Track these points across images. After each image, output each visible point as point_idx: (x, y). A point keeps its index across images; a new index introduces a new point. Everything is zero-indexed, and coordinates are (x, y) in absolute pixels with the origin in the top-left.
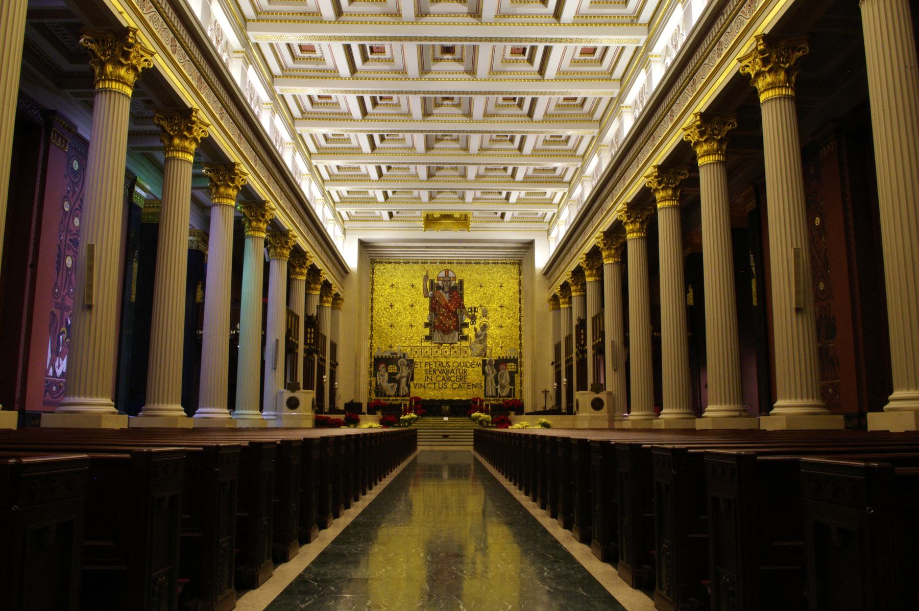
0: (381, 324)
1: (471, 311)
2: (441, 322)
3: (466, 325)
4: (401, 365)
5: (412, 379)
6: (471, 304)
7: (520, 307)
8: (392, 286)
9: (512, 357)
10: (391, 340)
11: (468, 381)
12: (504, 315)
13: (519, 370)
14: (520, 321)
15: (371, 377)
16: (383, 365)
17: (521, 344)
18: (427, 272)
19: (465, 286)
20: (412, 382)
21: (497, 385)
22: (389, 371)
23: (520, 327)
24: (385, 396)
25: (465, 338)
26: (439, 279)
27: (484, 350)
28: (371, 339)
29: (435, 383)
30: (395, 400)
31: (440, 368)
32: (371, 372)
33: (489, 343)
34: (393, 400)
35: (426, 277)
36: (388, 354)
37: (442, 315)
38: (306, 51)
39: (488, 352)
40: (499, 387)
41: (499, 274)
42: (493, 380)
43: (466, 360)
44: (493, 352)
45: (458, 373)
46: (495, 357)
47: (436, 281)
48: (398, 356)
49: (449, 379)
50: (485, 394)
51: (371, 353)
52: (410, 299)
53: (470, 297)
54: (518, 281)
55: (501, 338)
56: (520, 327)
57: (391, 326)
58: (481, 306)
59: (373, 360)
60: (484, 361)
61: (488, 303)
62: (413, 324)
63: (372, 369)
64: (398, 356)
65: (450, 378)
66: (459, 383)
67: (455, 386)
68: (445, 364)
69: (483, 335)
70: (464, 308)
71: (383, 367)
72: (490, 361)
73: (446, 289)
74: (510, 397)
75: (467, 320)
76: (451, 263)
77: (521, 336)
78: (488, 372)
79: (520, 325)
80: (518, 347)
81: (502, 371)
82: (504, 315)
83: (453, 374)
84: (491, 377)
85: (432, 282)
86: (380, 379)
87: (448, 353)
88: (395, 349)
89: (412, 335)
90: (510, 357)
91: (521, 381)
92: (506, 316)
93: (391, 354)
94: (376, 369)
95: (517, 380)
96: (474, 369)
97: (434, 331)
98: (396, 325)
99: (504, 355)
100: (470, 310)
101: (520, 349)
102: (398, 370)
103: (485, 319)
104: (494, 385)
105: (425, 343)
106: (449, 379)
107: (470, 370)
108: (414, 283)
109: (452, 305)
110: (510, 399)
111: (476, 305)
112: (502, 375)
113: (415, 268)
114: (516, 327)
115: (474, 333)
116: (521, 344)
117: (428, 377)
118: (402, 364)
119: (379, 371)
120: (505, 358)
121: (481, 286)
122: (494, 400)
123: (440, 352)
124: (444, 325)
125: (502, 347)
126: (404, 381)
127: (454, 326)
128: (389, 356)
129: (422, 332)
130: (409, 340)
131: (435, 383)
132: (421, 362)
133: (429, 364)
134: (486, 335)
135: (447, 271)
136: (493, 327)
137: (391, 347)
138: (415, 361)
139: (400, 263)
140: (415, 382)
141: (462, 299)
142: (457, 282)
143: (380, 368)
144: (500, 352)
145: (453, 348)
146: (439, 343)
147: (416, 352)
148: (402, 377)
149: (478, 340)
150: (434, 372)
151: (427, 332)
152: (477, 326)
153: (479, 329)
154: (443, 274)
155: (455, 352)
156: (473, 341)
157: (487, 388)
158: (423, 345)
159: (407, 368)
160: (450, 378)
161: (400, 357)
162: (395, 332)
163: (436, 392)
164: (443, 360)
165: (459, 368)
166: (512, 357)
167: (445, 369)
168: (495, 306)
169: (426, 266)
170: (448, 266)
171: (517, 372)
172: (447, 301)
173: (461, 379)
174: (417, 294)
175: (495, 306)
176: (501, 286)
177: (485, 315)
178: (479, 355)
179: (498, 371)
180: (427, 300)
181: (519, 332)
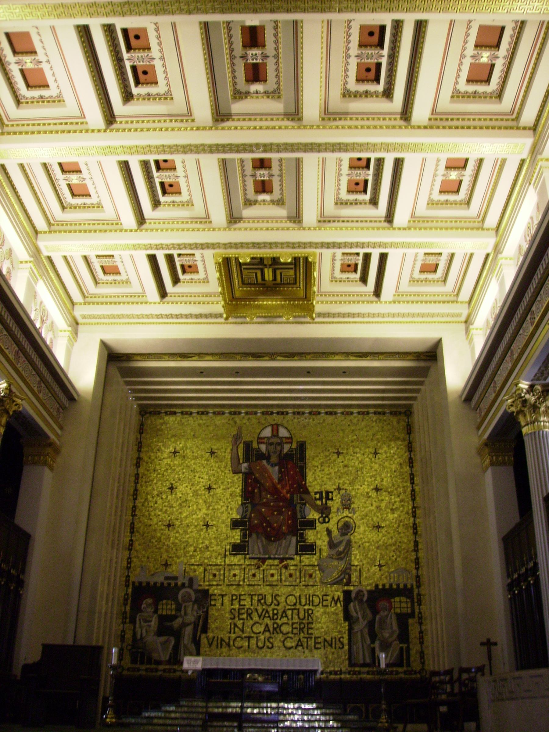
0: (150, 522)
1: (321, 499)
2: (263, 518)
3: (311, 524)
4: (184, 601)
5: (205, 630)
6: (321, 486)
7: (413, 490)
8: (175, 453)
9: (402, 586)
10: (167, 551)
11: (316, 633)
12: (383, 505)
13: (417, 611)
14: (414, 516)
15: (124, 623)
16: (150, 601)
17: (417, 559)
18: (240, 429)
19: (309, 453)
20: (203, 636)
21: (373, 642)
22: (160, 612)
23: (415, 527)
24: (149, 662)
25: (310, 549)
26: (260, 440)
27: (347, 572)
28: (130, 550)
29: (249, 638)
30: (170, 671)
31: (260, 609)
32: (125, 612)
33: (356, 558)
34: (164, 671)
35: (237, 438)
36: (160, 579)
37: (266, 505)
38: (79, 196)
39: (354, 578)
40: (377, 645)
41: (371, 433)
42: (366, 630)
44: (364, 575)
45: (295, 617)
46: (367, 585)
47: (255, 445)
48: (179, 583)
49: (277, 629)
50: (350, 659)
51: (128, 576)
52: (206, 477)
53: (318, 473)
54: (406, 443)
55: (378, 548)
56: (415, 527)
57: (169, 526)
58: (339, 489)
59: (130, 590)
60: (347, 594)
61: (352, 483)
62: (210, 523)
63: (128, 608)
64: (179, 583)
65: (280, 626)
66: (297, 638)
67: (289, 644)
68: (269, 599)
69: (344, 544)
70: (307, 492)
71: (150, 605)
72: (359, 592)
73: (274, 459)
74: (400, 665)
75: (314, 515)
76: (282, 413)
77: (416, 543)
78: (354, 614)
79: (415, 524)
80: (413, 565)
81: (383, 614)
82: (383, 505)
83: (285, 620)
84: (361, 625)
85: (248, 446)
86: (141, 627)
87: (276, 578)
89: (207, 542)
90: (398, 585)
91: (421, 632)
92: (386, 507)
93: (167, 578)
94: (136, 607)
95: (414, 632)
96: (329, 610)
97: (250, 536)
98: (177, 523)
99: (385, 581)
100: (318, 496)
101: (417, 569)
102: (178, 609)
103: (346, 513)
104: (368, 642)
105: (232, 558)
106: (277, 629)
107: (319, 611)
108: (214, 447)
109: (283, 487)
110: (400, 669)
111: (330, 487)
112: (382, 622)
113: (217, 423)
114: (406, 526)
115: (326, 539)
116: (417, 559)
117: (235, 625)
118: (188, 598)
119: (142, 611)
120: (387, 586)
121: (338, 453)
122: (368, 673)
123: (259, 576)
124: (269, 525)
125: (380, 566)
126: (189, 630)
127: (288, 526)
128: (162, 584)
129: (227, 537)
130: (201, 551)
131: (249, 638)
132: (223, 596)
133: (239, 598)
134: (349, 543)
135: (275, 428)
136: (362, 529)
137: (166, 565)
138: (211, 592)
139: (191, 413)
140: (211, 635)
141: (303, 476)
142: (294, 446)
143: (143, 606)
144: (378, 575)
145: (286, 567)
146: (259, 559)
147: (215, 575)
148: (184, 625)
149: (334, 552)
150: (249, 615)
151: (236, 536)
152: (332, 525)
153: (335, 532)
154: (267, 433)
155: (291, 575)
156: (325, 554)
157: (354, 648)
158: (227, 562)
159: (196, 607)
160: (280, 626)
161: (183, 585)
162: (176, 538)
163: (249, 655)
164: (266, 590)
165: (298, 606)
166: (402, 586)
167: (270, 609)
168: (365, 488)
169: (237, 418)
170: (278, 419)
171: (412, 615)
172: (276, 480)
173: (301, 630)
174: (218, 467)
175: (365, 488)
176: (376, 453)
177: (347, 505)
178: (338, 582)
179: (375, 611)
180: (238, 479)
181: (412, 537)
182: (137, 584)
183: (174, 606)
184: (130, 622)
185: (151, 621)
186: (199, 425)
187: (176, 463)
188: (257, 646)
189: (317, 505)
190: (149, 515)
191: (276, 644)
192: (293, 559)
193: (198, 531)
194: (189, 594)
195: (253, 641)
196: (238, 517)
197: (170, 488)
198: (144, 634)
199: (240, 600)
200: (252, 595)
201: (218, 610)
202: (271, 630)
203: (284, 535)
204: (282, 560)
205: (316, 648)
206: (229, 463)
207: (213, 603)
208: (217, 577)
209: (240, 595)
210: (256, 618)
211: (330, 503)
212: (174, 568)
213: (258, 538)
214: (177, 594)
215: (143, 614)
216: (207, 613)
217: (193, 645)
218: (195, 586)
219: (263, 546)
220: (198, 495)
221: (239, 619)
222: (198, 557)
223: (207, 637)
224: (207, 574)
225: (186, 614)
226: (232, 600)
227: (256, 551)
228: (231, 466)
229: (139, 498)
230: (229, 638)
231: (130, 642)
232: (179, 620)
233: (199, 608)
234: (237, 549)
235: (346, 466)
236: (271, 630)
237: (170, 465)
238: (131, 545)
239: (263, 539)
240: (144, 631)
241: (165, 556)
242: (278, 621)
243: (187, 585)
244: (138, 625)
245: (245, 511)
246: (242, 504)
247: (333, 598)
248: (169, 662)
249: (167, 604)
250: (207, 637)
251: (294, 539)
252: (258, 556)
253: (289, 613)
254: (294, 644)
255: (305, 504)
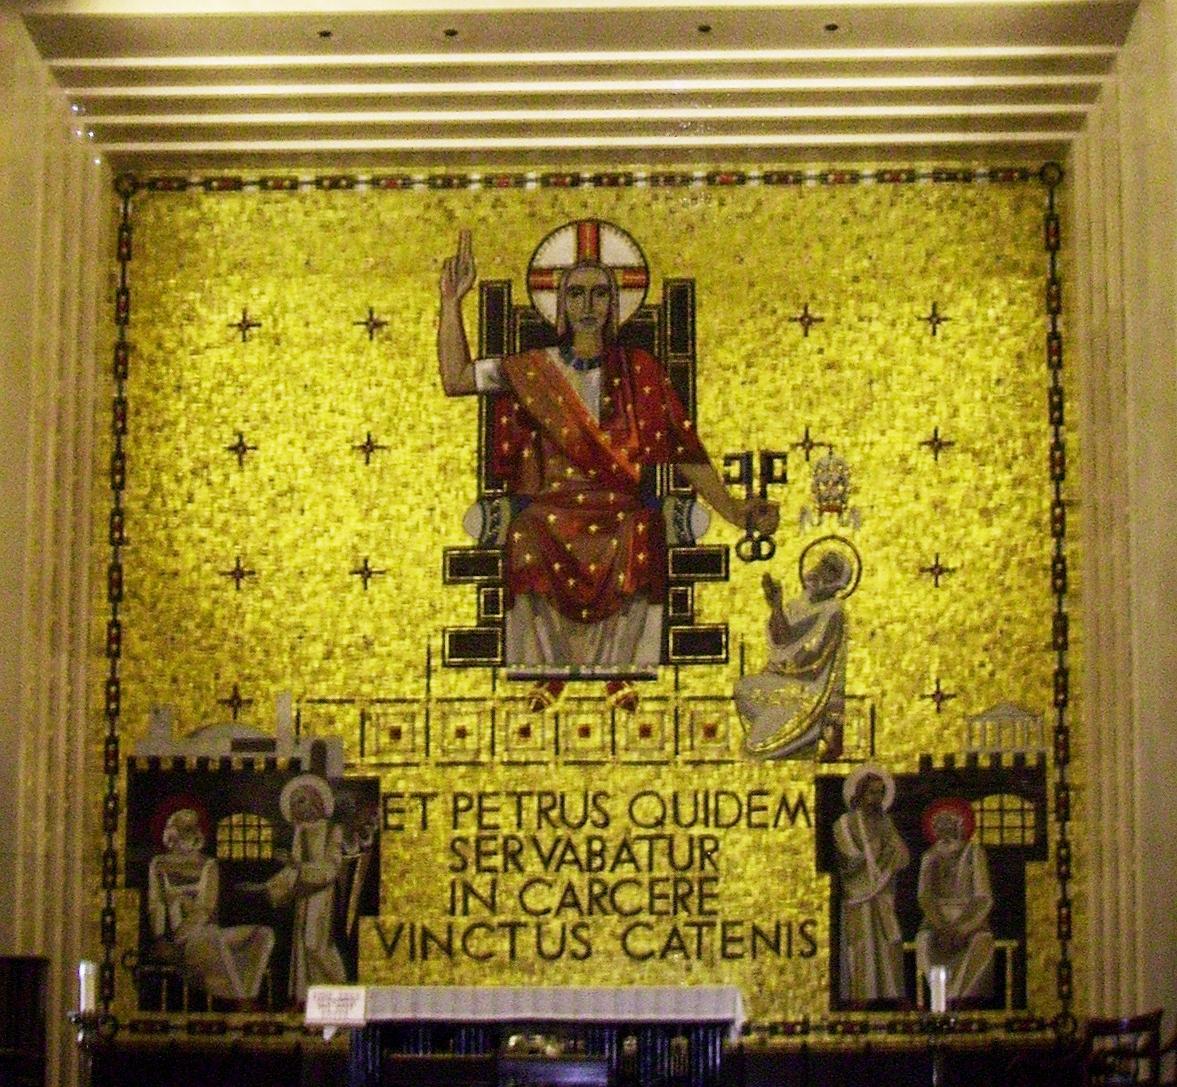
1: (746, 478)
2: (551, 546)
3: (713, 564)
4: (299, 817)
5: (371, 904)
8: (245, 325)
15: (109, 886)
16: (187, 816)
20: (366, 923)
22: (223, 851)
24: (199, 1002)
25: (708, 644)
26: (539, 281)
28: (115, 655)
29: (513, 927)
31: (546, 838)
32: (111, 854)
35: (457, 271)
36: (216, 748)
37: (562, 501)
43: (712, 779)
45: (662, 860)
47: (519, 296)
48: (282, 761)
49: (603, 899)
52: (355, 409)
57: (238, 574)
58: (808, 444)
59: (122, 784)
61: (850, 424)
62: (376, 563)
64: (282, 761)
66: (666, 927)
67: (640, 943)
68: (575, 809)
70: (699, 456)
73: (586, 343)
75: (719, 532)
76: (613, 181)
83: (627, 870)
86: (166, 900)
87: (595, 739)
88: (263, 718)
89: (367, 628)
93: (239, 745)
97: (510, 603)
98: (265, 565)
100: (735, 470)
102: (282, 841)
105: (452, 676)
107: (736, 844)
109: (617, 442)
111: (776, 439)
113: (386, 217)
117: (468, 889)
119: (164, 850)
121: (807, 322)
123: (542, 733)
124: (573, 567)
126: (318, 907)
127: (637, 572)
129: (434, 611)
131: (513, 927)
132: (424, 798)
137: (236, 702)
138: (385, 787)
139: (295, 185)
140: (390, 919)
141: (685, 400)
142: (655, 296)
146: (541, 679)
147: (396, 734)
148: (304, 890)
150: (512, 857)
151: (463, 607)
154: (561, 251)
158: (437, 691)
159: (338, 833)
161: (295, 766)
162: (264, 614)
163: (514, 980)
165: (669, 828)
167: (578, 838)
172: (594, 418)
173: (680, 900)
180: (465, 414)
182: (143, 765)
183: (267, 833)
184: (128, 885)
185: (196, 880)
186: (325, 226)
187: (252, 360)
188: (540, 952)
189: (732, 501)
190: (170, 539)
191: (598, 945)
192: (649, 677)
193: (335, 590)
194: (316, 793)
195: (527, 938)
196: (469, 542)
197: (233, 449)
198: (177, 921)
199: (481, 811)
200: (520, 796)
201: (410, 843)
202: (584, 902)
203: (623, 601)
204: (615, 682)
205: (725, 956)
206: (433, 359)
207: (393, 820)
208: (405, 742)
209: (482, 796)
210: (533, 865)
211: (775, 492)
212: (262, 710)
213: (535, 612)
214: (277, 793)
215: (169, 858)
216: (374, 854)
217: (335, 951)
218: (334, 770)
219: (552, 637)
220: (329, 471)
221: (481, 870)
222: (339, 677)
223: (379, 927)
224: (371, 732)
225: (307, 856)
226: (456, 811)
227: (531, 654)
228: (441, 371)
229: (131, 482)
230: (450, 929)
231: (134, 945)
232: (289, 876)
233: (349, 838)
234: (468, 648)
235: (830, 366)
236: (584, 902)
237: (229, 370)
238: (115, 639)
239: (554, 615)
240: (175, 910)
241: (229, 672)
242: (605, 875)
243: (306, 765)
244: (153, 893)
245: (491, 523)
246: (481, 499)
247: (784, 802)
248: (259, 1004)
249: (245, 827)
250: (379, 927)
251: (655, 615)
252: (539, 670)
253: (641, 849)
254: (656, 945)
255: (693, 497)
